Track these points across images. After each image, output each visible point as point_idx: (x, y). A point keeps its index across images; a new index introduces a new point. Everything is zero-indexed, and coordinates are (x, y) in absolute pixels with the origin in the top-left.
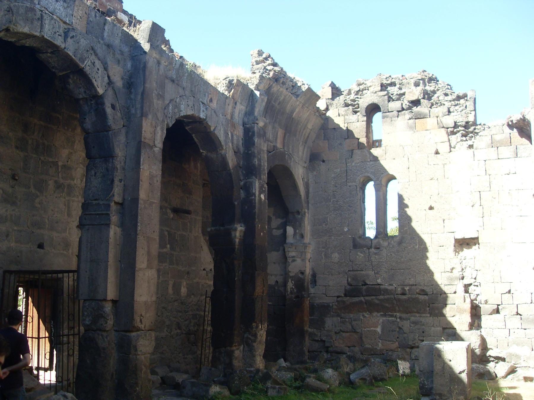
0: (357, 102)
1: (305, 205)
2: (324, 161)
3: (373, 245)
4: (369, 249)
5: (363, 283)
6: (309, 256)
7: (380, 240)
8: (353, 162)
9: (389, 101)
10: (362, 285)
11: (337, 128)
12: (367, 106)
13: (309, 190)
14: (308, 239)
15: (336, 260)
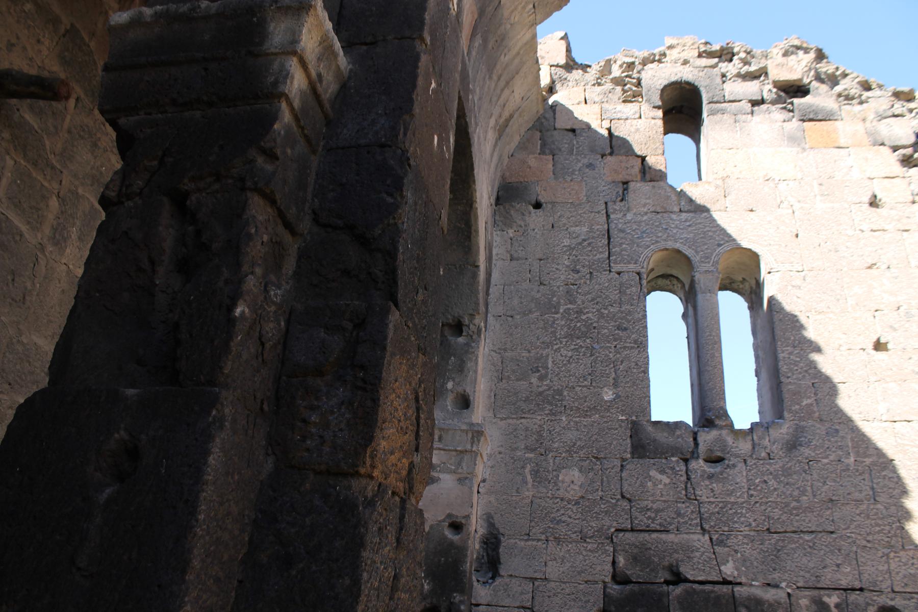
0: (628, 86)
1: (482, 308)
2: (538, 205)
3: (702, 448)
4: (686, 461)
5: (668, 576)
6: (481, 470)
7: (724, 432)
8: (628, 210)
9: (724, 82)
10: (667, 583)
11: (578, 130)
12: (665, 87)
13: (490, 275)
14: (479, 413)
15: (575, 492)
